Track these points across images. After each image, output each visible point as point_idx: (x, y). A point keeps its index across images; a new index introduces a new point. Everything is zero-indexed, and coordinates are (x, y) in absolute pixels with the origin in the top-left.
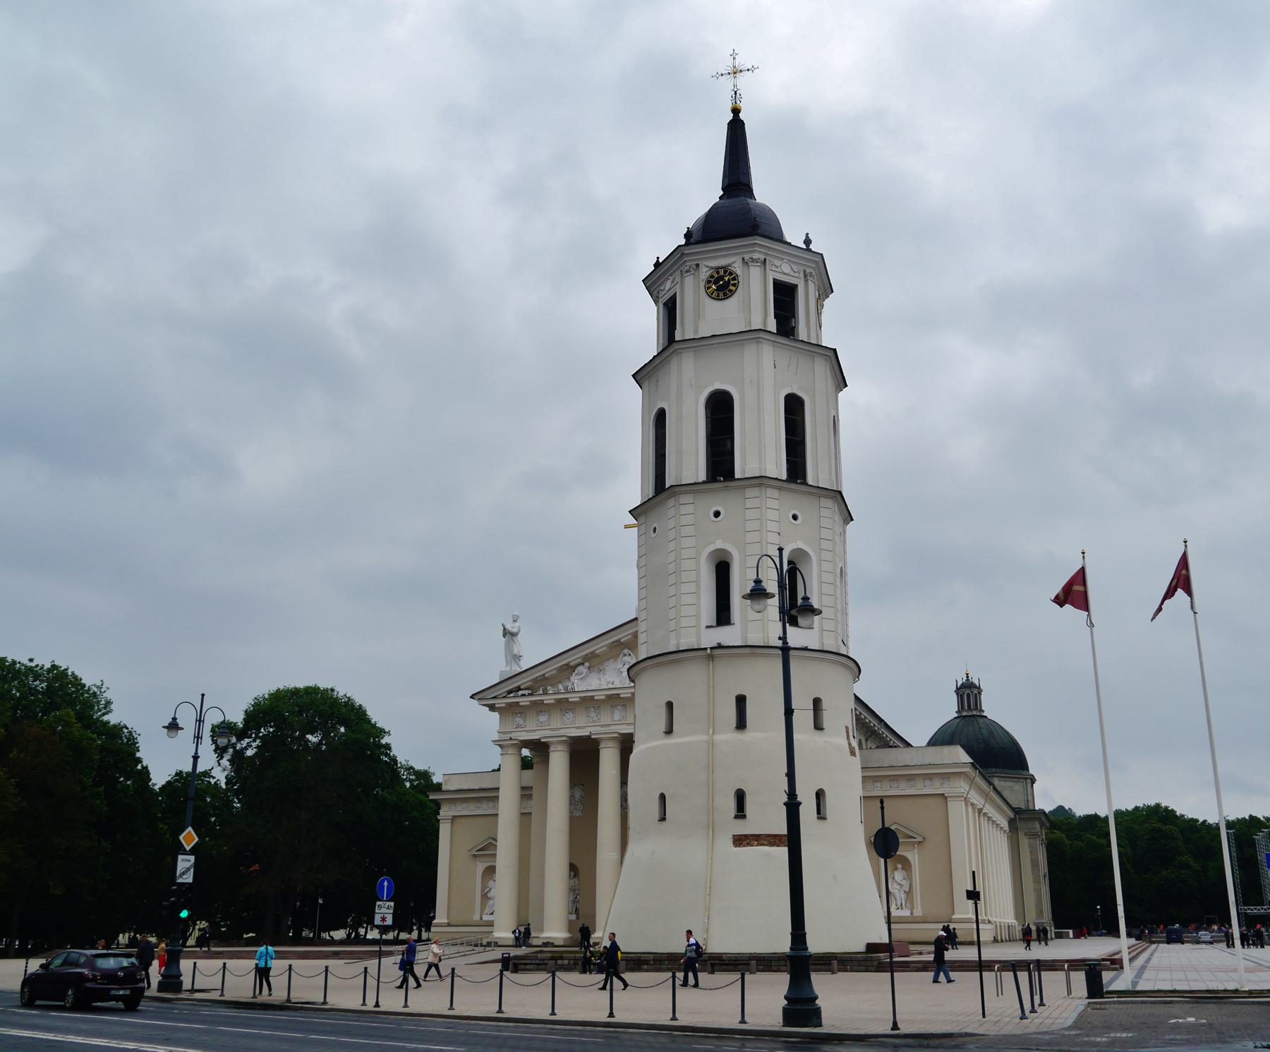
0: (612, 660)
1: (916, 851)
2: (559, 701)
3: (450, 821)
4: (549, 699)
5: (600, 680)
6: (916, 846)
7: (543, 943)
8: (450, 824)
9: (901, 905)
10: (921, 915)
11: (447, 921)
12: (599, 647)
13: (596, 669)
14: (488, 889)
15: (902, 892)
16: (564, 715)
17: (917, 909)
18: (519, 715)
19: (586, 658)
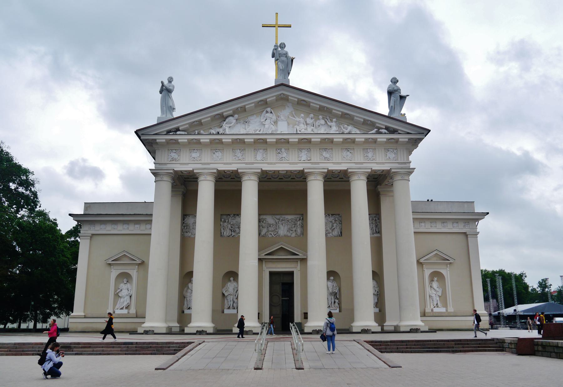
0: (255, 116)
1: (448, 270)
2: (212, 142)
3: (89, 238)
4: (205, 139)
5: (246, 130)
6: (448, 265)
7: (197, 331)
8: (89, 240)
9: (437, 304)
10: (453, 311)
11: (84, 314)
12: (249, 104)
13: (242, 121)
14: (119, 290)
15: (437, 296)
16: (214, 153)
17: (450, 307)
18: (174, 151)
19: (236, 112)
